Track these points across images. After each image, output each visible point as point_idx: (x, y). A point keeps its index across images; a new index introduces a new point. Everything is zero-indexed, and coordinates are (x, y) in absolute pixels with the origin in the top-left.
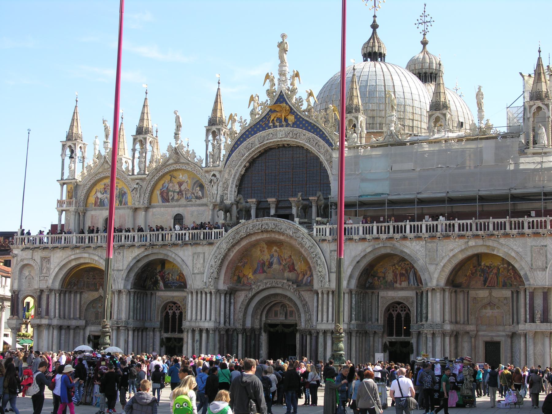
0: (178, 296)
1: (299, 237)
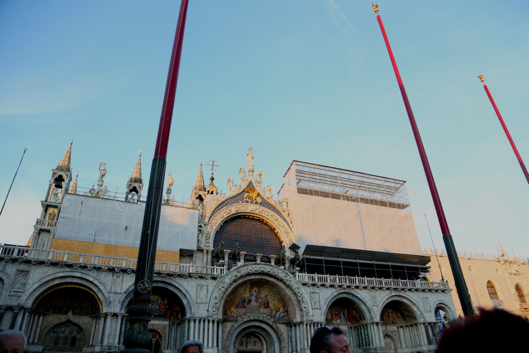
0: (159, 325)
1: (288, 280)
